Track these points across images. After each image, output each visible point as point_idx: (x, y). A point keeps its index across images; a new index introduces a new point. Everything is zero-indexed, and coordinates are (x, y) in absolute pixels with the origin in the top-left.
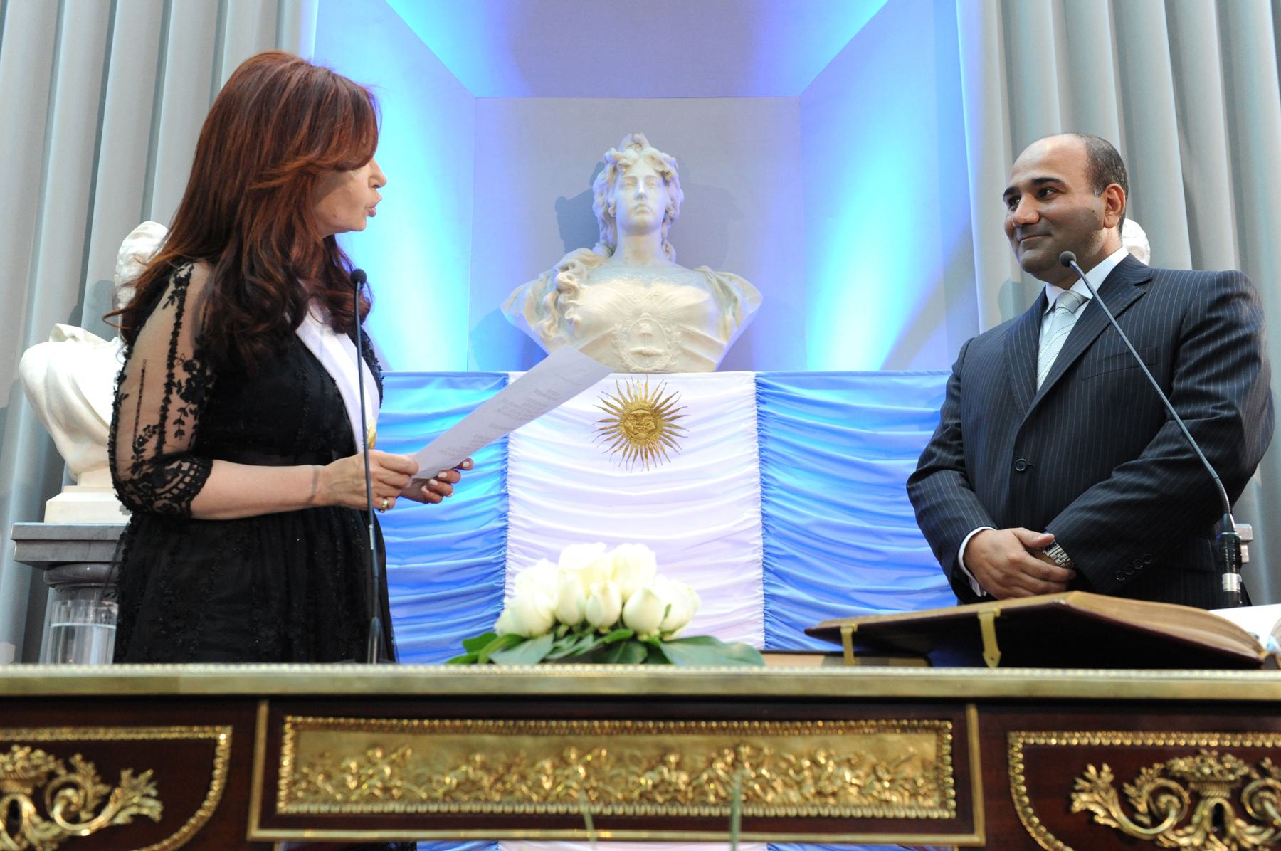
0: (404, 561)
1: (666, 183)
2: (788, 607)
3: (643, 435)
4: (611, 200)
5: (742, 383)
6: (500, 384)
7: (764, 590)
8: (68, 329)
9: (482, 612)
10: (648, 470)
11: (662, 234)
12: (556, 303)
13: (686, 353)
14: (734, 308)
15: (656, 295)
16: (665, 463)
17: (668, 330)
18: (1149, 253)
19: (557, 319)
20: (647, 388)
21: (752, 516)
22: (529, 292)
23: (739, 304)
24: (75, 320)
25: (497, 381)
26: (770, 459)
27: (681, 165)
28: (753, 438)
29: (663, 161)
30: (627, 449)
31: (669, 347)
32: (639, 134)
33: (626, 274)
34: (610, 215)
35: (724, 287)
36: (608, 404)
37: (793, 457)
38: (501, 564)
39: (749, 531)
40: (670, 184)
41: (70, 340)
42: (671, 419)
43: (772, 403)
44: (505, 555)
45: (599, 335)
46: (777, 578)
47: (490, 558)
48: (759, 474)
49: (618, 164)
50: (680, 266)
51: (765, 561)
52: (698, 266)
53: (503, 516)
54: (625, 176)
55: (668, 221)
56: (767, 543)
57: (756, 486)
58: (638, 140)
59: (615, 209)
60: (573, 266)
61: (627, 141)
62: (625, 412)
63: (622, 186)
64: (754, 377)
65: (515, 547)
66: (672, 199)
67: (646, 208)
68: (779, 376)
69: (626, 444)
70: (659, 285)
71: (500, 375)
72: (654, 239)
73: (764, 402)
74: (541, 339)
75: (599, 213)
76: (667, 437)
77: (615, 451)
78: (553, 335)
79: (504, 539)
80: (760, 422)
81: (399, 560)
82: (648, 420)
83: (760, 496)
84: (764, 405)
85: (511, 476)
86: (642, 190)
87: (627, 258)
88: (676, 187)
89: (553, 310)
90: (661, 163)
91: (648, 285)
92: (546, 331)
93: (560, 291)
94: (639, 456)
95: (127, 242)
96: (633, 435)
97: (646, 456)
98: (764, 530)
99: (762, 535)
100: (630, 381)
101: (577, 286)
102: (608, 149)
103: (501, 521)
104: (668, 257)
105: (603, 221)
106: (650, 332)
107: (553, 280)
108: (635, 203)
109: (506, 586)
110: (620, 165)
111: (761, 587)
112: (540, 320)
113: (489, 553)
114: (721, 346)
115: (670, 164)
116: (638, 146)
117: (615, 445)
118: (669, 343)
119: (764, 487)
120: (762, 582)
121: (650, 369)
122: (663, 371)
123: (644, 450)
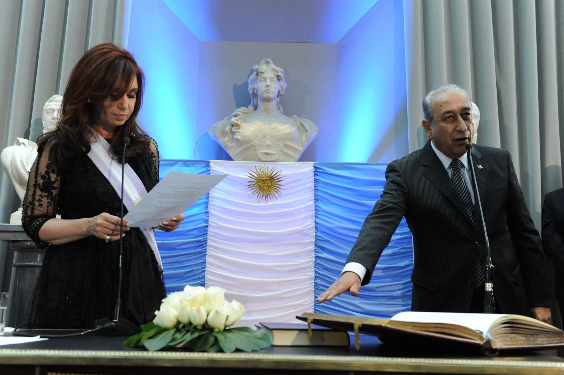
0: (165, 239)
1: (279, 80)
2: (323, 261)
3: (266, 188)
4: (256, 87)
5: (308, 167)
6: (206, 165)
7: (315, 254)
8: (22, 140)
9: (197, 261)
10: (268, 203)
11: (277, 102)
12: (231, 131)
13: (285, 153)
14: (306, 134)
15: (273, 128)
16: (275, 200)
17: (277, 143)
18: (480, 117)
19: (231, 138)
20: (268, 168)
21: (310, 223)
22: (220, 125)
23: (308, 132)
24: (26, 136)
25: (204, 165)
26: (319, 199)
27: (286, 72)
28: (313, 190)
29: (278, 71)
30: (259, 194)
31: (278, 151)
32: (268, 58)
33: (261, 119)
34: (255, 93)
35: (302, 125)
36: (251, 175)
37: (330, 199)
38: (205, 241)
39: (309, 229)
40: (281, 81)
41: (22, 145)
42: (278, 182)
43: (320, 175)
44: (207, 238)
45: (248, 145)
46: (321, 250)
47: (201, 239)
48: (314, 205)
49: (258, 72)
50: (285, 116)
51: (316, 242)
52: (292, 116)
53: (206, 221)
54: (262, 77)
55: (280, 96)
56: (317, 234)
57: (313, 211)
58: (268, 61)
59: (257, 91)
60: (239, 115)
61: (263, 61)
62: (259, 178)
63: (260, 81)
64: (313, 164)
65: (211, 234)
66: (281, 87)
67: (270, 91)
68: (324, 164)
69: (259, 192)
70: (275, 124)
71: (206, 162)
72: (273, 104)
73: (317, 175)
74: (224, 146)
75: (251, 92)
76: (276, 189)
77: (254, 195)
78: (229, 144)
79: (207, 231)
80: (315, 183)
81: (163, 239)
82: (268, 182)
83: (314, 215)
84: (317, 176)
85: (210, 204)
86: (268, 83)
87: (262, 112)
88: (283, 82)
89: (230, 134)
90: (277, 72)
91: (270, 124)
92: (227, 143)
93: (233, 126)
94: (264, 197)
95: (47, 103)
96: (261, 188)
97: (267, 197)
98: (316, 229)
99: (315, 231)
100: (261, 165)
101: (240, 124)
102: (255, 65)
103: (205, 223)
104: (279, 111)
105: (252, 96)
106: (270, 144)
107: (230, 120)
108: (265, 89)
109: (207, 251)
110: (259, 72)
111: (314, 253)
112: (225, 138)
113: (199, 237)
114: (299, 151)
115: (281, 72)
116: (268, 63)
117: (254, 192)
118: (278, 149)
119: (316, 211)
120: (314, 251)
121: (270, 160)
122: (275, 161)
123: (266, 194)
